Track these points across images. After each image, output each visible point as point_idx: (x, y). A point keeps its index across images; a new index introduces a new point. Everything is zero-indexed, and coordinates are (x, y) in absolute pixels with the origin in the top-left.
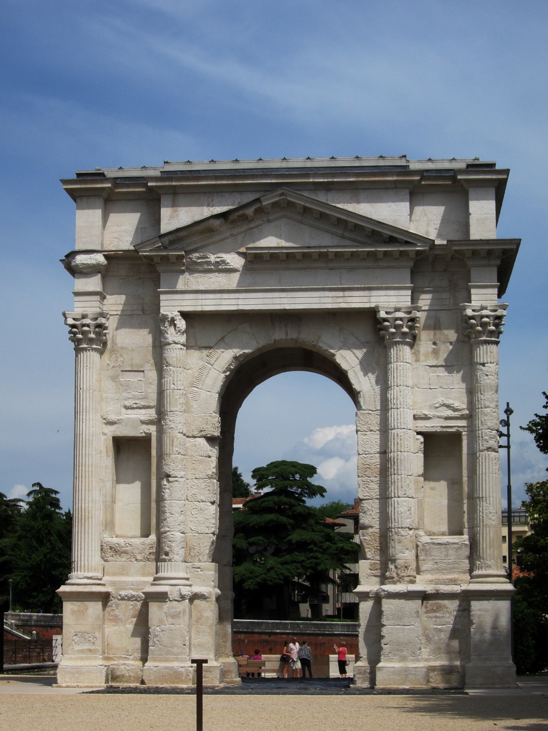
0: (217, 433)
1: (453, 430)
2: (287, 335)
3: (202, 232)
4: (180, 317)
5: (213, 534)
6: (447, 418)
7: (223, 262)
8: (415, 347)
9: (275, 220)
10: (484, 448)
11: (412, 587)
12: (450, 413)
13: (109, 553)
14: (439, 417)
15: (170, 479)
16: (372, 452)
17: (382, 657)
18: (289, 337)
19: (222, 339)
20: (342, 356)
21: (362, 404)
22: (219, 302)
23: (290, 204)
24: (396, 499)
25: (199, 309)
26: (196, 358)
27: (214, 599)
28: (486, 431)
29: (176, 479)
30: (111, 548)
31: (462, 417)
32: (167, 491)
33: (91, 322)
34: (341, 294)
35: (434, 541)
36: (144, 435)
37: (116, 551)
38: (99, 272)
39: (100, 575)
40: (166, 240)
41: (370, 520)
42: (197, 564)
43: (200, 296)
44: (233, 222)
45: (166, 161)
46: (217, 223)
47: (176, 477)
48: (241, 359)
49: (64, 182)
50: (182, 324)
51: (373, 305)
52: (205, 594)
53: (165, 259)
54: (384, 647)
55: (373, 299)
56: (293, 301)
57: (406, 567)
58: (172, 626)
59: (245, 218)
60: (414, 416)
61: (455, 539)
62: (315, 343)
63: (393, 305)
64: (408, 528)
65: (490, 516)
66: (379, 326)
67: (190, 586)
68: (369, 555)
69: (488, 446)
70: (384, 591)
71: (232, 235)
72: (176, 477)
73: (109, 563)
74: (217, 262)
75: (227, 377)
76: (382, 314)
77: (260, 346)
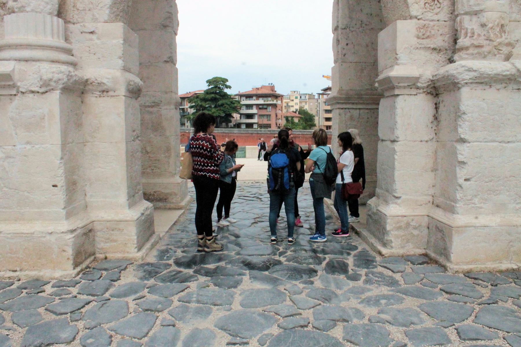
27: (122, 91)
42: (90, 27)
52: (105, 81)
57: (502, 26)
58: (28, 147)
67: (74, 65)
68: (415, 10)
70: (470, 70)
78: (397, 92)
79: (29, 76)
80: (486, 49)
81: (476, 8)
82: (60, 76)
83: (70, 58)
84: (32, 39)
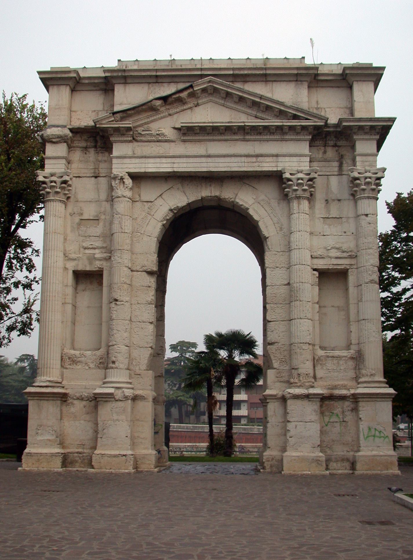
0: (155, 268)
1: (343, 267)
2: (211, 193)
3: (145, 111)
4: (128, 177)
5: (151, 347)
6: (337, 258)
7: (163, 135)
8: (312, 202)
9: (204, 103)
10: (368, 280)
11: (312, 391)
12: (339, 254)
13: (67, 362)
14: (331, 258)
15: (117, 302)
16: (278, 284)
17: (288, 448)
18: (213, 195)
19: (160, 196)
20: (254, 210)
21: (270, 247)
22: (158, 165)
23: (216, 91)
24: (298, 320)
25: (143, 170)
26: (139, 210)
27: (151, 399)
28: (370, 267)
29: (122, 303)
30: (69, 358)
31: (351, 257)
32: (115, 312)
33: (57, 179)
34: (254, 159)
35: (328, 354)
36: (97, 269)
37: (74, 361)
38: (65, 142)
39: (60, 380)
40: (118, 116)
41: (277, 337)
43: (143, 160)
44: (170, 104)
45: (119, 59)
46: (159, 103)
47: (123, 301)
48: (175, 212)
49: (39, 73)
50: (129, 181)
51: (279, 169)
53: (117, 130)
54: (290, 439)
55: (280, 164)
56: (217, 165)
59: (180, 101)
60: (311, 256)
61: (344, 353)
62: (233, 200)
63: (296, 169)
64: (308, 343)
65: (374, 334)
66: (284, 185)
67: (133, 389)
68: (276, 364)
69: (371, 279)
70: (289, 393)
71: (170, 115)
72: (123, 301)
73: (67, 370)
74: (157, 134)
75: (163, 225)
76: (287, 175)
77: (190, 201)
78: (268, 401)
79: (119, 394)
80: (299, 384)
81: (296, 367)
82: (131, 394)
83: (130, 386)
84: (120, 380)
